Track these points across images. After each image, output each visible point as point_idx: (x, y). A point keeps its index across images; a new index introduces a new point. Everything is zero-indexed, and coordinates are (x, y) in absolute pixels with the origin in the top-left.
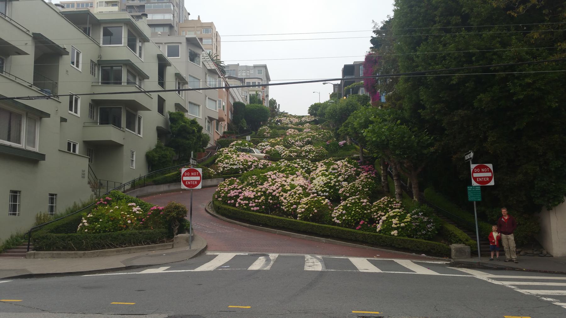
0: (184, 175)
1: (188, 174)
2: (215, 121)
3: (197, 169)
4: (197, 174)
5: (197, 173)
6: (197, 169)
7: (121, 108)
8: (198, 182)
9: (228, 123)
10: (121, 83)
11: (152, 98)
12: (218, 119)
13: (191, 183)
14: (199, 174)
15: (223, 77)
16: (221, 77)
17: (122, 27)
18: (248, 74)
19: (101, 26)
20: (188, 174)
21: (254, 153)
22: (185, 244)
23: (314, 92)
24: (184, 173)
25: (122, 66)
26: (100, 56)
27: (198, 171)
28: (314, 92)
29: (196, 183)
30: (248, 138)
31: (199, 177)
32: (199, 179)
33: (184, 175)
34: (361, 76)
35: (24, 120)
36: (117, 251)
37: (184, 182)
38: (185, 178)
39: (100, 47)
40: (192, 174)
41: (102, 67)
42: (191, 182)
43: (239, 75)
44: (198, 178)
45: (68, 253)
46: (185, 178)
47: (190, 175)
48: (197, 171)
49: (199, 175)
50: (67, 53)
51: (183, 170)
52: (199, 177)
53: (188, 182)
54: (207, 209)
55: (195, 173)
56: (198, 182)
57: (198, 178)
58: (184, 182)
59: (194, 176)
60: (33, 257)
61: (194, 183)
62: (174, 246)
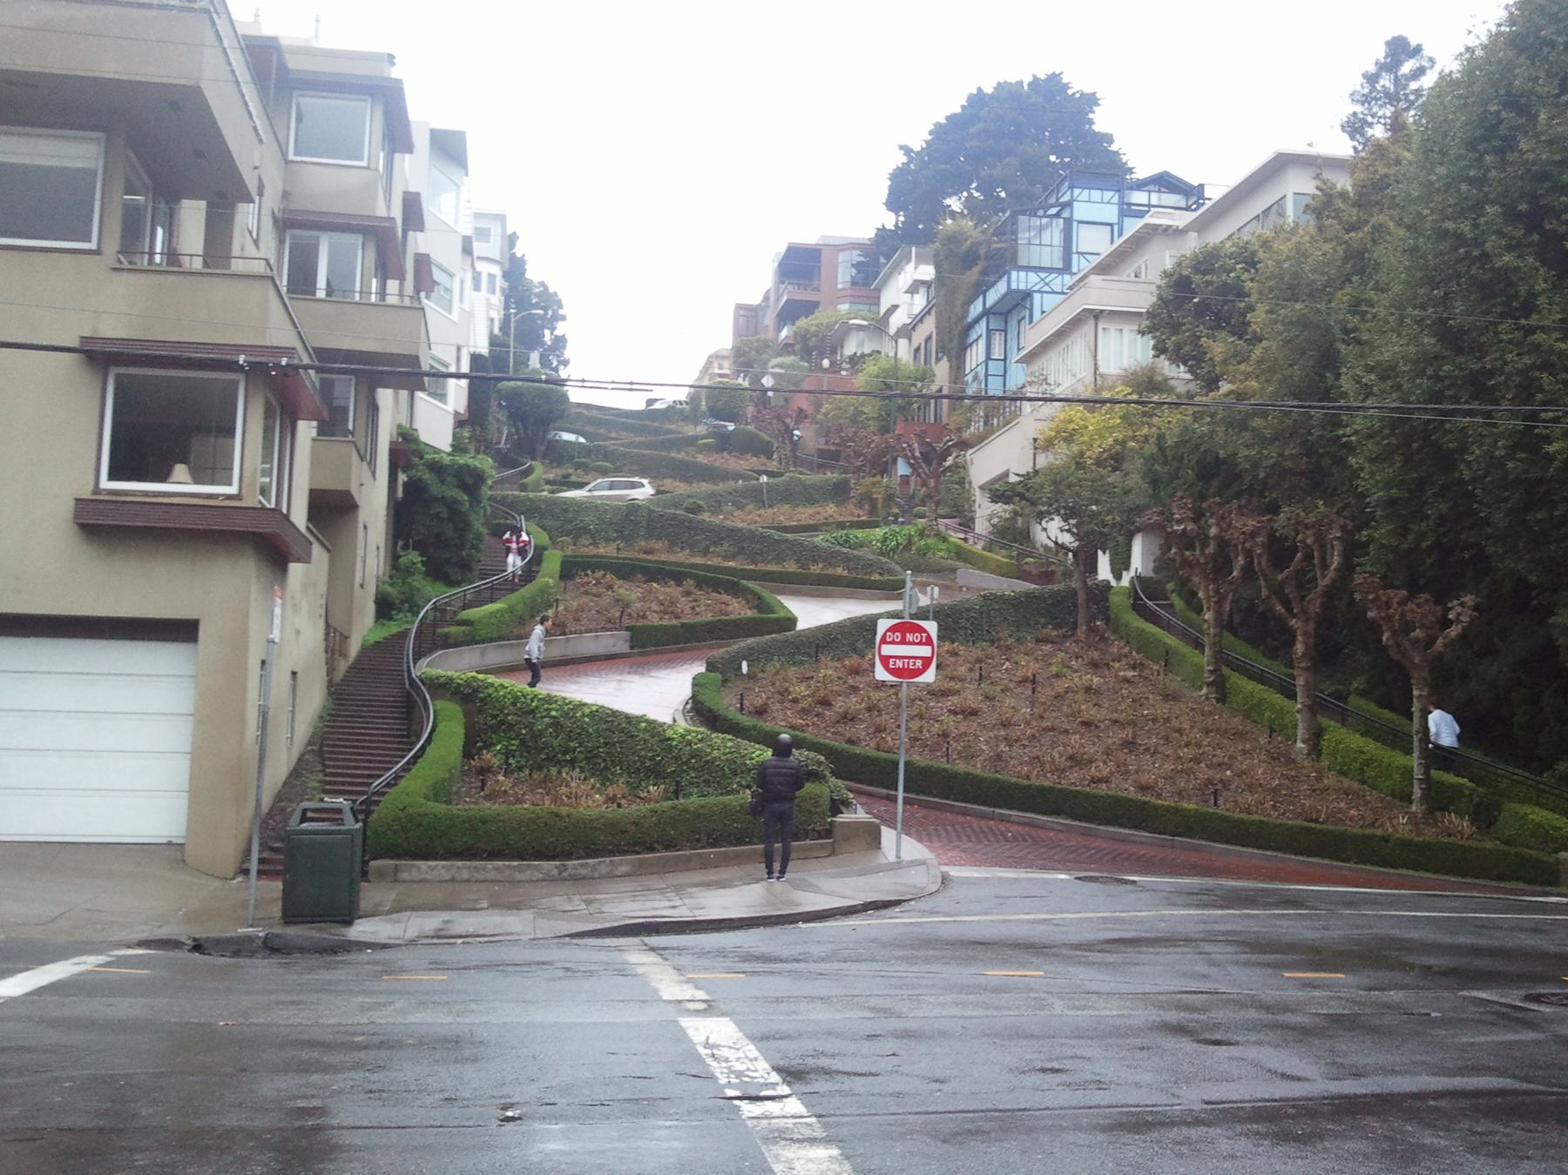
0: (883, 641)
3: (923, 623)
6: (923, 623)
8: (927, 662)
27: (924, 630)
29: (919, 663)
32: (929, 655)
33: (883, 641)
37: (885, 660)
38: (888, 650)
39: (287, 162)
40: (909, 637)
44: (925, 651)
45: (509, 867)
46: (888, 650)
47: (903, 642)
48: (922, 630)
52: (929, 648)
56: (927, 662)
57: (925, 651)
58: (885, 660)
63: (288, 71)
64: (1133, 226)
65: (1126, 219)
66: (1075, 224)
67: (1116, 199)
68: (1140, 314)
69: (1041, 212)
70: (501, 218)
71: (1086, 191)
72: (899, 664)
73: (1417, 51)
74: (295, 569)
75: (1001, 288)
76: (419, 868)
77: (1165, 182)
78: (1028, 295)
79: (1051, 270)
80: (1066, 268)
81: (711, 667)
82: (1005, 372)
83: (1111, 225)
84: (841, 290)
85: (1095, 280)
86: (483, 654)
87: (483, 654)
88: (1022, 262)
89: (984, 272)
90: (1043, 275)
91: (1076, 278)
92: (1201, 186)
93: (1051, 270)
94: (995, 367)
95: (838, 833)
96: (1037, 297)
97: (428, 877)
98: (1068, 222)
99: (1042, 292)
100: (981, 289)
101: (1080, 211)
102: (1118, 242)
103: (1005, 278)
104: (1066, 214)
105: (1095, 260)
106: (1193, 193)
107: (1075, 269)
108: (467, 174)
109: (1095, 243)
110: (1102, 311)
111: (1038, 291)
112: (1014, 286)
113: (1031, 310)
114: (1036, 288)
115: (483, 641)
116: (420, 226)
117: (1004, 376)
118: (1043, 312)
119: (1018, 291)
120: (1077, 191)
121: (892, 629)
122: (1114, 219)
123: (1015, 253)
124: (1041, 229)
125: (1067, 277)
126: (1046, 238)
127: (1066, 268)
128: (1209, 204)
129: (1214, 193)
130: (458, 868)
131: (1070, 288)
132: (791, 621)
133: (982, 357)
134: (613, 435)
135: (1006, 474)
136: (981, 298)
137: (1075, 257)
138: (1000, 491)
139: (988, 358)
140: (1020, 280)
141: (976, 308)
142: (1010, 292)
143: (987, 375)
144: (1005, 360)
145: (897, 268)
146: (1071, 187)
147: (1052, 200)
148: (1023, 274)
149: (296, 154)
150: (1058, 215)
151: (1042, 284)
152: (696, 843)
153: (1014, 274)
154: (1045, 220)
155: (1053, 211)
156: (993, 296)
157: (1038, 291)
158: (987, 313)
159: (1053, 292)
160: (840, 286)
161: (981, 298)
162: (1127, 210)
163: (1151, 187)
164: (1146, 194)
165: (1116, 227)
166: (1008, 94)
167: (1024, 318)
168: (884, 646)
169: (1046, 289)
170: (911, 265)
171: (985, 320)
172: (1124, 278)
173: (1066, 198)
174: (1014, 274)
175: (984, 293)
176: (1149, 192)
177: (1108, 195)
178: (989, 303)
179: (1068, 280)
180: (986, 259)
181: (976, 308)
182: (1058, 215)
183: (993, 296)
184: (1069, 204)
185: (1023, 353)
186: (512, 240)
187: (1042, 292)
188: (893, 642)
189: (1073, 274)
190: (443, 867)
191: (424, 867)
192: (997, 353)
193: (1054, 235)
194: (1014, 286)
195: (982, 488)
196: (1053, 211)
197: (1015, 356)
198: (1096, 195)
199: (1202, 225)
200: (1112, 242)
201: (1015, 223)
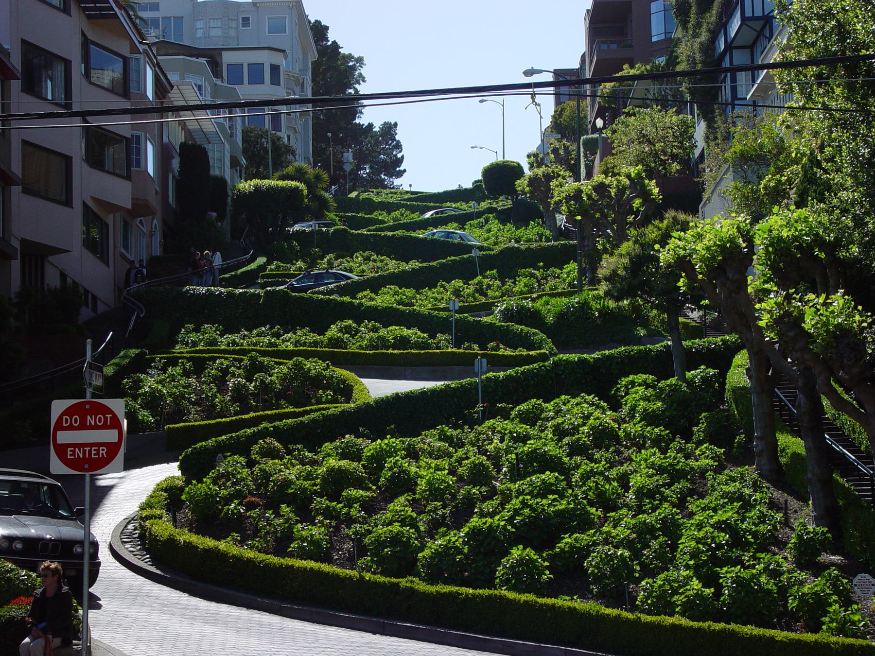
1: (76, 419)
2: (118, 215)
4: (106, 419)
5: (109, 416)
9: (164, 222)
12: (129, 205)
13: (84, 452)
15: (146, 47)
16: (141, 48)
18: (233, 33)
20: (76, 418)
24: (60, 419)
27: (111, 412)
29: (103, 451)
31: (116, 431)
32: (115, 439)
33: (59, 426)
34: (654, 39)
37: (62, 450)
38: (63, 437)
42: (87, 449)
43: (199, 34)
44: (111, 436)
46: (63, 437)
47: (83, 426)
48: (108, 410)
49: (115, 424)
51: (59, 407)
52: (116, 431)
53: (74, 451)
54: (115, 548)
55: (100, 418)
58: (62, 450)
59: (96, 427)
61: (98, 454)
72: (79, 453)
84: (655, 42)
112: (748, 14)
119: (754, 18)
121: (69, 412)
136: (722, 31)
142: (744, 19)
160: (654, 39)
161: (722, 31)
168: (60, 434)
188: (71, 428)
194: (748, 14)
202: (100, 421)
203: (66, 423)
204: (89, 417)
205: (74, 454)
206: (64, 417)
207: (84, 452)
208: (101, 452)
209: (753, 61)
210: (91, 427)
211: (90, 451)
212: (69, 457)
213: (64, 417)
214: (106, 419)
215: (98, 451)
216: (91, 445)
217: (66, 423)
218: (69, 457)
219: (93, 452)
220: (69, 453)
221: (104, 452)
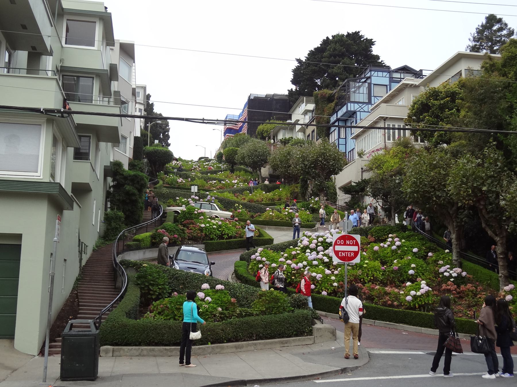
0: (336, 244)
1: (342, 241)
3: (354, 236)
4: (353, 242)
5: (354, 241)
6: (354, 236)
7: (90, 137)
8: (356, 253)
10: (91, 100)
11: (122, 126)
13: (345, 254)
14: (357, 242)
17: (95, 22)
19: (64, 18)
20: (342, 241)
21: (217, 210)
22: (331, 338)
23: (214, 130)
24: (336, 241)
25: (93, 78)
26: (61, 61)
27: (355, 239)
28: (214, 130)
29: (352, 254)
30: (194, 188)
32: (357, 250)
33: (336, 244)
35: (60, 149)
36: (236, 347)
39: (62, 47)
40: (348, 242)
41: (63, 76)
42: (346, 253)
44: (355, 248)
45: (166, 349)
47: (345, 244)
48: (354, 239)
50: (51, 54)
53: (342, 254)
55: (351, 242)
56: (356, 253)
57: (355, 248)
58: (337, 253)
59: (350, 245)
60: (111, 354)
61: (351, 255)
62: (317, 341)
63: (63, 9)
64: (395, 86)
65: (392, 83)
66: (372, 85)
67: (388, 76)
68: (402, 119)
69: (358, 81)
70: (144, 88)
71: (376, 72)
72: (343, 254)
73: (500, 21)
74: (66, 212)
75: (344, 109)
76: (124, 350)
77: (405, 70)
78: (354, 113)
79: (363, 103)
80: (370, 102)
81: (242, 259)
82: (346, 143)
83: (386, 86)
85: (383, 105)
86: (144, 253)
87: (144, 253)
88: (352, 100)
89: (336, 105)
90: (360, 105)
91: (373, 106)
92: (421, 71)
93: (363, 103)
94: (342, 141)
95: (315, 333)
96: (358, 113)
97: (127, 354)
98: (370, 84)
99: (360, 112)
100: (335, 111)
101: (375, 80)
102: (389, 93)
103: (345, 107)
104: (369, 81)
105: (381, 99)
106: (418, 74)
107: (373, 103)
108: (134, 62)
109: (381, 93)
110: (387, 118)
111: (359, 111)
112: (349, 109)
113: (356, 118)
114: (358, 110)
115: (144, 248)
116: (117, 79)
117: (346, 145)
118: (361, 119)
119: (351, 111)
120: (373, 72)
121: (340, 238)
122: (387, 83)
123: (349, 97)
124: (359, 87)
125: (370, 106)
126: (361, 90)
127: (370, 102)
128: (425, 77)
129: (427, 73)
130: (142, 350)
131: (372, 110)
132: (271, 241)
133: (336, 137)
134: (231, 137)
135: (350, 182)
136: (336, 114)
137: (373, 98)
138: (347, 189)
139: (339, 137)
140: (351, 107)
141: (333, 119)
142: (347, 111)
143: (339, 144)
144: (346, 138)
145: (298, 106)
146: (370, 71)
147: (363, 76)
148: (352, 104)
149: (66, 44)
150: (365, 82)
151: (360, 108)
152: (250, 337)
153: (349, 104)
154: (360, 84)
155: (363, 80)
156: (340, 113)
157: (359, 111)
158: (338, 120)
159: (365, 112)
161: (336, 114)
162: (392, 80)
163: (400, 71)
164: (399, 74)
165: (388, 86)
166: (338, 39)
167: (353, 121)
169: (362, 110)
170: (304, 104)
171: (337, 122)
172: (394, 104)
173: (368, 75)
174: (349, 104)
175: (337, 112)
176: (401, 73)
177: (385, 74)
178: (339, 116)
179: (371, 107)
180: (337, 99)
181: (333, 119)
182: (365, 82)
183: (340, 113)
184: (369, 78)
185: (353, 136)
186: (148, 97)
187: (360, 112)
188: (340, 245)
189: (372, 105)
190: (135, 349)
191: (126, 350)
192: (342, 135)
193: (364, 89)
194: (349, 109)
195: (340, 188)
196: (363, 80)
197: (349, 137)
198: (380, 74)
199: (425, 84)
200: (387, 93)
201: (349, 86)
202: (351, 243)
203: (339, 243)
204: (347, 241)
205: (341, 255)
206: (338, 240)
207: (345, 254)
208: (352, 254)
209: (346, 125)
210: (348, 245)
211: (348, 254)
212: (340, 256)
213: (338, 240)
214: (353, 242)
215: (351, 254)
216: (348, 252)
217: (339, 243)
218: (340, 256)
219: (349, 254)
220: (340, 254)
221: (353, 255)
